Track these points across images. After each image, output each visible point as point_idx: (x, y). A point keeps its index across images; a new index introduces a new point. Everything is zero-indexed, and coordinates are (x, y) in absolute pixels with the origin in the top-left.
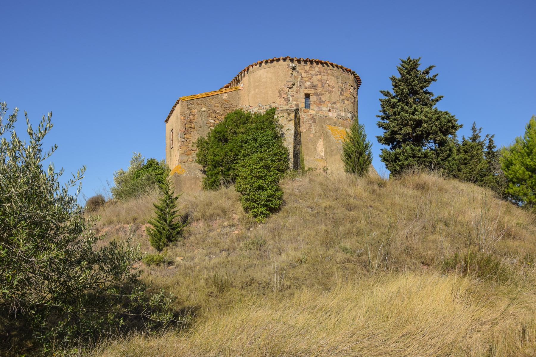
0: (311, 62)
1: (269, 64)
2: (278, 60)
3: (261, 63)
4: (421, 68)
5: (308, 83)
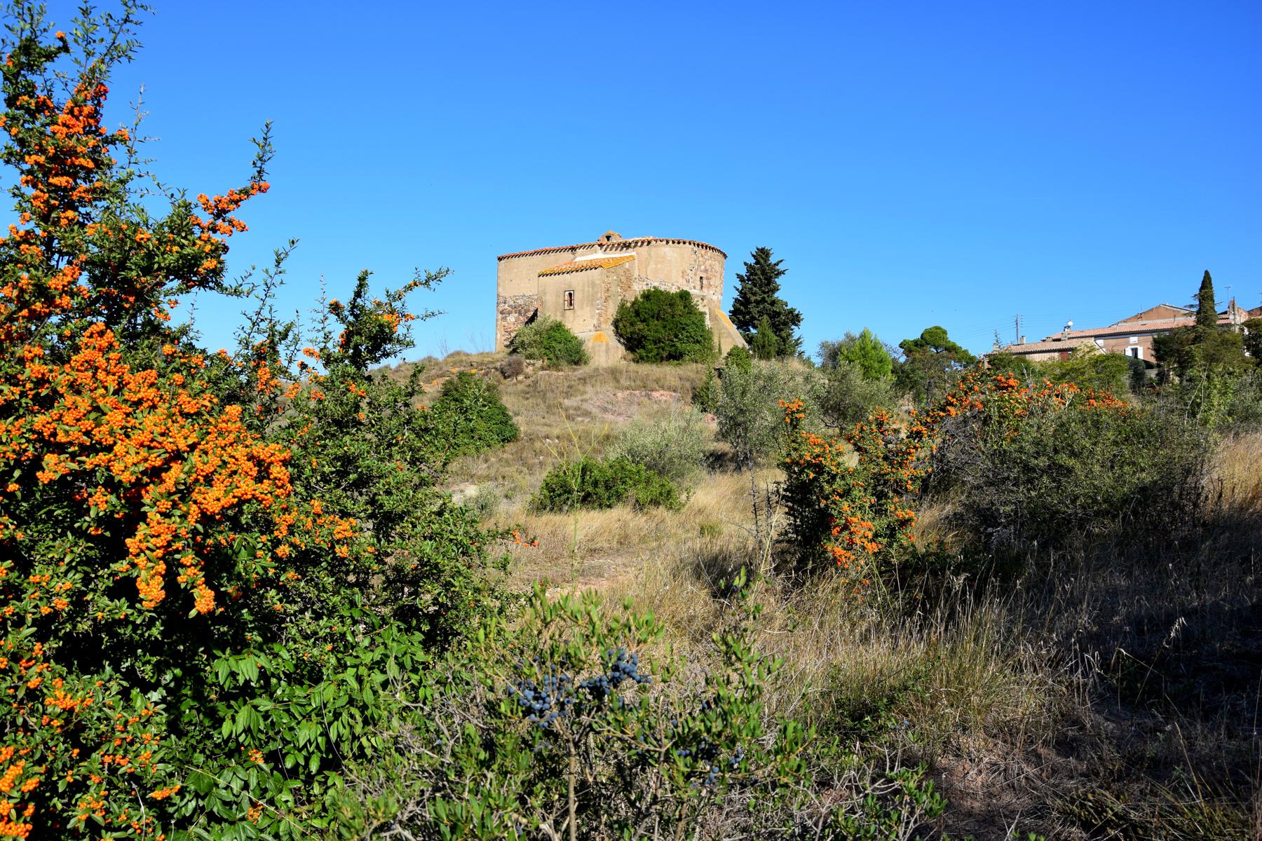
2: (684, 243)
3: (668, 242)
4: (773, 260)
5: (703, 267)
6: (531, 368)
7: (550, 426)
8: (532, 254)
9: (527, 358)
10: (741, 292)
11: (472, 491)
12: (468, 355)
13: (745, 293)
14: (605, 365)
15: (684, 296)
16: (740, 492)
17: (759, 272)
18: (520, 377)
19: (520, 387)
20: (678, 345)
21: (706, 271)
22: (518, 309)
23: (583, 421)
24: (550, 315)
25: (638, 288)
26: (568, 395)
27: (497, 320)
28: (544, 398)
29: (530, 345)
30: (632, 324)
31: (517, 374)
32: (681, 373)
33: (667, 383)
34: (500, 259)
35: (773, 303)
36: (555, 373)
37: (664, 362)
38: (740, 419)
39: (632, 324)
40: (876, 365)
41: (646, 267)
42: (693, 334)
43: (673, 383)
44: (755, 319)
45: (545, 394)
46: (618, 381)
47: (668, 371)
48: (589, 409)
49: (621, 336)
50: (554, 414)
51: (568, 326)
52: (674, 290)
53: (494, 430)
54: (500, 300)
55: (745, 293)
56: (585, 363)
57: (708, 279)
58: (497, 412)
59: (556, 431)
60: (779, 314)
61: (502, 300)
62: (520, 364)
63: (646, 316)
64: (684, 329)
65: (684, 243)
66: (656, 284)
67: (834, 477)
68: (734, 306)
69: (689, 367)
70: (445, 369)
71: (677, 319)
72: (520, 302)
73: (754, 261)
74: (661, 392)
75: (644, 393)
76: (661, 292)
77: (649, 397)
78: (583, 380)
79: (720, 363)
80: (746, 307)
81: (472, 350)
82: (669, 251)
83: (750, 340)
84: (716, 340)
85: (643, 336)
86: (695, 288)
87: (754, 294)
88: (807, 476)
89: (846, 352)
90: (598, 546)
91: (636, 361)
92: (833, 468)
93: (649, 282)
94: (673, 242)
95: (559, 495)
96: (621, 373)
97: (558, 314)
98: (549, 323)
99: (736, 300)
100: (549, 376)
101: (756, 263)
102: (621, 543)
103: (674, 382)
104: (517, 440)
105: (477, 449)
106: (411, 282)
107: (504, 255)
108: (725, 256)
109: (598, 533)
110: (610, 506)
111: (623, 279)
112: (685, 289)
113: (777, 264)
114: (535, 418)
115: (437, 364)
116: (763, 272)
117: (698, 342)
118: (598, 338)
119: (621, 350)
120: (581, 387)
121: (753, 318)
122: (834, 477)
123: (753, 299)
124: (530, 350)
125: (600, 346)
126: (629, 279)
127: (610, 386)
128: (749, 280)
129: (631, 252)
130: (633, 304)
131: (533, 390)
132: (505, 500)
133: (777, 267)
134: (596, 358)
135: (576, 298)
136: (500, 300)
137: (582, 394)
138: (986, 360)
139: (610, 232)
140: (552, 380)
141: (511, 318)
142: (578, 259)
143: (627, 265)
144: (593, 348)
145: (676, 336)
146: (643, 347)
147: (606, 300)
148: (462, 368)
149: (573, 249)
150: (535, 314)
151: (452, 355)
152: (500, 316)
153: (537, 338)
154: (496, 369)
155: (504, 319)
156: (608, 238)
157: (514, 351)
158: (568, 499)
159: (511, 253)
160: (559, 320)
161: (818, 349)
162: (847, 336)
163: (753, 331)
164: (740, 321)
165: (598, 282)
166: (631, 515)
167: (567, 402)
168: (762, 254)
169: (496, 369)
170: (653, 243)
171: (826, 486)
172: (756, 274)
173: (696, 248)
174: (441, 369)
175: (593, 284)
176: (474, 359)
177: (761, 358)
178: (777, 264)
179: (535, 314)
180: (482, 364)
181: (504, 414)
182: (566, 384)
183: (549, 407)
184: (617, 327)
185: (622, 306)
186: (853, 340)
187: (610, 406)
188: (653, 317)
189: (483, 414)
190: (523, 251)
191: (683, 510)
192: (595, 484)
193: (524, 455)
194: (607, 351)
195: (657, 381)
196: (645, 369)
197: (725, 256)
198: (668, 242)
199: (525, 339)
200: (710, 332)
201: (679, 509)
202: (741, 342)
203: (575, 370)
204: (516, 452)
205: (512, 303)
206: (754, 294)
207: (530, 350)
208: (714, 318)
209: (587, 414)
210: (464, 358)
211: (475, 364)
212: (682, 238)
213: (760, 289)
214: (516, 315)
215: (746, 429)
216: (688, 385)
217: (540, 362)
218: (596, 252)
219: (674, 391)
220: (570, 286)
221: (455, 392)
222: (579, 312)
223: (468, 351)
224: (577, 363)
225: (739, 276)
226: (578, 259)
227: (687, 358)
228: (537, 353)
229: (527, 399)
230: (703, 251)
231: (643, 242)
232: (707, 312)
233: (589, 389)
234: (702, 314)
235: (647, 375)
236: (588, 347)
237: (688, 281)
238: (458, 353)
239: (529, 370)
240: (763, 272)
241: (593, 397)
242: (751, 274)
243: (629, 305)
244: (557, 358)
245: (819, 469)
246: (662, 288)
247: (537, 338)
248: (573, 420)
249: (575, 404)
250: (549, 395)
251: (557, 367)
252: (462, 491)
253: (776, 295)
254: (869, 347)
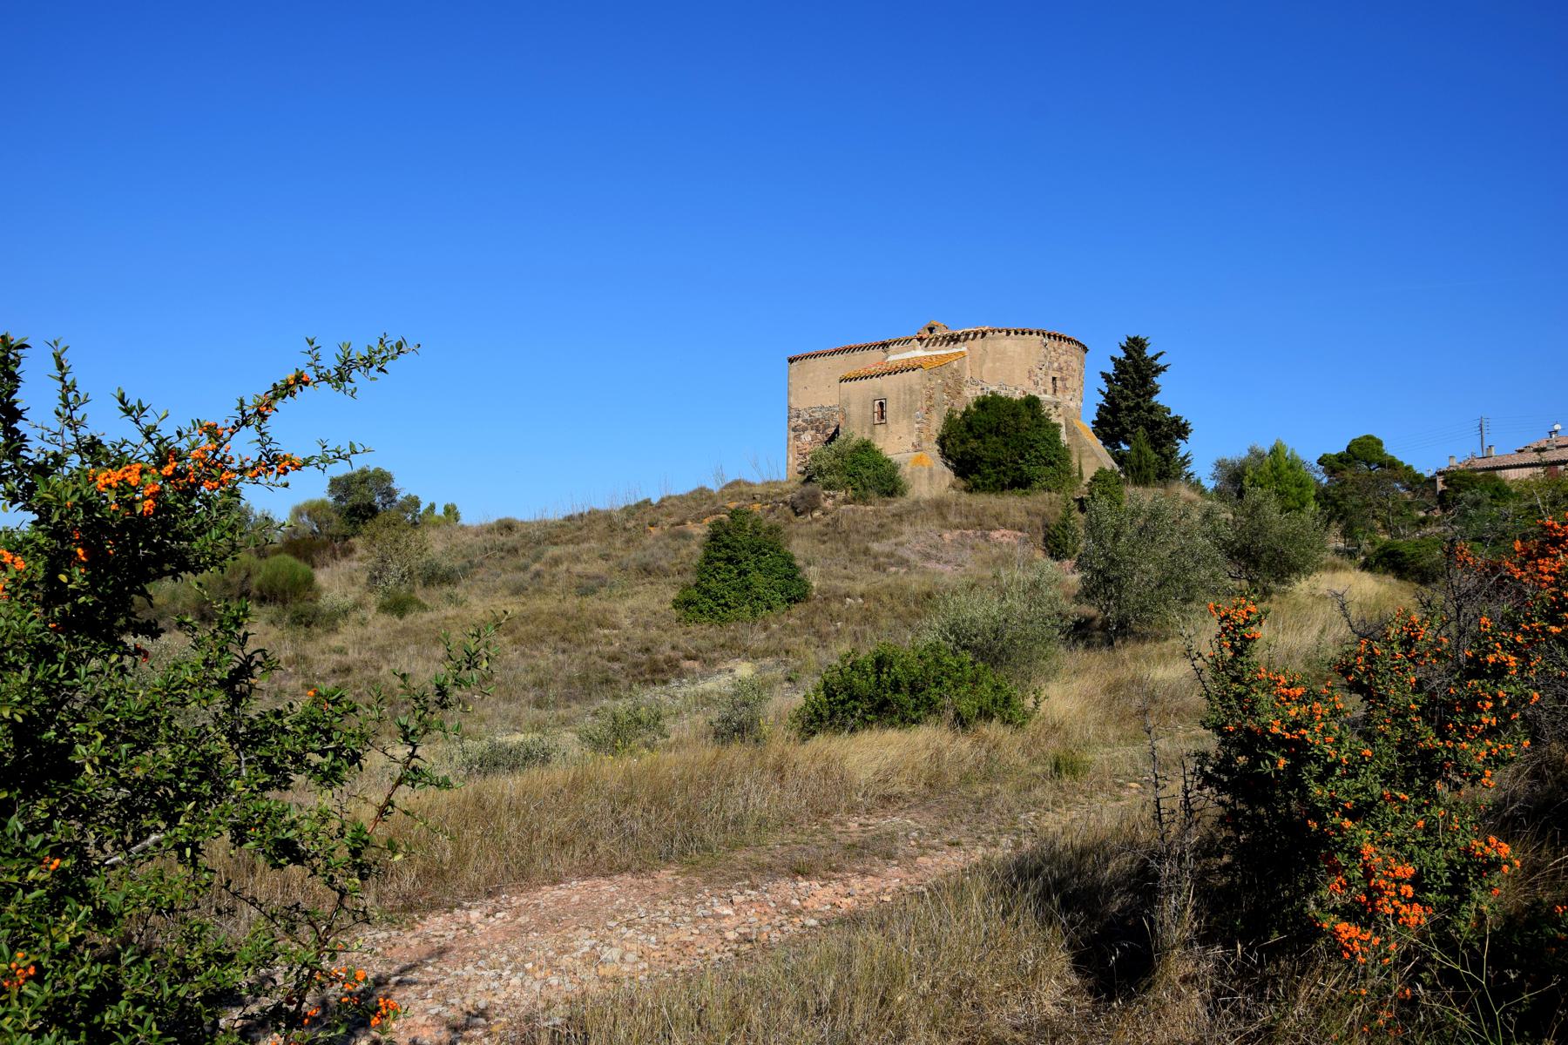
0: (1060, 337)
1: (1019, 335)
2: (1031, 333)
3: (1008, 333)
4: (1149, 352)
5: (1056, 365)
6: (830, 501)
7: (853, 579)
8: (832, 353)
9: (825, 488)
10: (1107, 396)
11: (744, 670)
12: (750, 485)
13: (1113, 398)
14: (927, 496)
15: (1032, 403)
16: (1114, 689)
17: (1131, 369)
18: (817, 514)
19: (817, 527)
20: (1025, 468)
21: (1060, 369)
23: (896, 573)
24: (856, 432)
25: (971, 394)
26: (877, 536)
27: (788, 439)
28: (846, 542)
29: (829, 471)
30: (963, 442)
31: (813, 509)
32: (1030, 505)
33: (1010, 520)
34: (791, 361)
35: (1152, 409)
36: (862, 507)
37: (1006, 491)
38: (1113, 574)
39: (963, 442)
40: (1294, 490)
41: (981, 366)
42: (1044, 453)
43: (1018, 519)
44: (1127, 431)
45: (848, 536)
46: (945, 518)
47: (1012, 504)
48: (906, 556)
49: (949, 457)
50: (858, 563)
51: (878, 445)
52: (1018, 396)
53: (777, 587)
54: (792, 413)
55: (1113, 398)
56: (902, 494)
57: (1063, 379)
58: (781, 562)
59: (860, 587)
60: (1159, 424)
61: (794, 413)
62: (815, 496)
63: (982, 431)
64: (1031, 447)
65: (1031, 333)
66: (994, 388)
67: (1330, 769)
68: (1098, 415)
69: (1040, 498)
70: (720, 503)
71: (1022, 433)
72: (818, 415)
73: (1124, 355)
74: (1003, 531)
75: (979, 533)
76: (1001, 399)
77: (985, 537)
78: (899, 517)
79: (1082, 491)
80: (1115, 416)
81: (756, 479)
82: (1011, 345)
83: (1120, 459)
84: (1075, 460)
85: (980, 459)
86: (1045, 392)
87: (1126, 399)
88: (1274, 763)
89: (1251, 474)
90: (896, 789)
91: (969, 490)
92: (1328, 748)
93: (984, 385)
94: (1016, 333)
95: (843, 702)
96: (949, 506)
97: (866, 430)
98: (854, 441)
99: (1101, 407)
100: (854, 512)
101: (1127, 358)
102: (931, 785)
103: (1020, 518)
104: (808, 600)
105: (754, 613)
106: (291, 376)
107: (796, 354)
108: (1085, 349)
109: (894, 770)
110: (916, 722)
111: (950, 382)
112: (1033, 393)
113: (1155, 358)
114: (833, 568)
115: (710, 497)
116: (1137, 369)
117: (1051, 463)
118: (918, 460)
119: (949, 476)
120: (895, 526)
121: (1124, 431)
122: (1330, 769)
123: (1124, 404)
124: (829, 478)
125: (920, 471)
126: (959, 382)
127: (934, 525)
128: (1118, 379)
129: (961, 348)
130: (964, 415)
131: (833, 531)
132: (786, 685)
133: (1156, 362)
134: (916, 486)
135: (890, 409)
136: (792, 413)
137: (896, 536)
138: (1440, 479)
139: (934, 322)
140: (858, 517)
141: (807, 437)
142: (891, 358)
143: (955, 365)
144: (912, 473)
145: (1022, 457)
146: (979, 472)
147: (928, 410)
148: (742, 502)
149: (885, 345)
150: (837, 431)
151: (730, 485)
152: (792, 434)
153: (838, 461)
154: (785, 503)
155: (797, 438)
156: (931, 330)
157: (809, 479)
158: (855, 708)
159: (806, 352)
160: (866, 438)
161: (1212, 470)
162: (1252, 451)
163: (1125, 447)
164: (1106, 434)
165: (917, 387)
166: (949, 736)
167: (876, 547)
168: (1135, 346)
169: (785, 503)
171: (1316, 790)
172: (1127, 372)
173: (1046, 340)
174: (714, 503)
175: (911, 391)
176: (758, 490)
177: (1136, 483)
178: (1155, 358)
179: (837, 431)
180: (767, 496)
181: (791, 565)
182: (877, 522)
183: (853, 553)
184: (943, 445)
185: (950, 418)
186: (1260, 456)
187: (934, 552)
188: (990, 431)
189: (763, 565)
190: (820, 350)
191: (1029, 726)
192: (896, 686)
193: (817, 620)
194: (931, 476)
195: (997, 517)
196: (981, 500)
197: (1085, 349)
198: (1008, 333)
199: (822, 463)
200: (1067, 450)
201: (1022, 724)
202: (1109, 463)
203: (888, 503)
204: (805, 616)
205: (807, 417)
206: (1126, 399)
207: (829, 478)
208: (1073, 432)
209: (903, 562)
210: (745, 489)
211: (758, 497)
212: (1028, 327)
213: (1133, 391)
214: (813, 432)
215: (1120, 588)
216: (1038, 521)
217: (843, 493)
219: (1020, 530)
220: (881, 393)
221: (725, 537)
222: (893, 427)
223: (750, 479)
224: (891, 494)
225: (1105, 376)
226: (891, 358)
227: (1037, 485)
228: (839, 482)
229: (824, 542)
230: (1056, 344)
231: (976, 334)
232: (1063, 423)
233: (906, 528)
234: (1056, 426)
235: (984, 509)
236: (905, 472)
237: (1036, 384)
238: (737, 483)
239: (829, 504)
240: (1137, 369)
241: (912, 539)
242: (1121, 372)
243: (958, 416)
244: (865, 488)
245: (1299, 752)
246: (1003, 393)
247: (838, 461)
248: (885, 570)
249: (887, 549)
250: (854, 536)
251: (865, 500)
252: (731, 671)
253: (1155, 399)
254: (1284, 467)
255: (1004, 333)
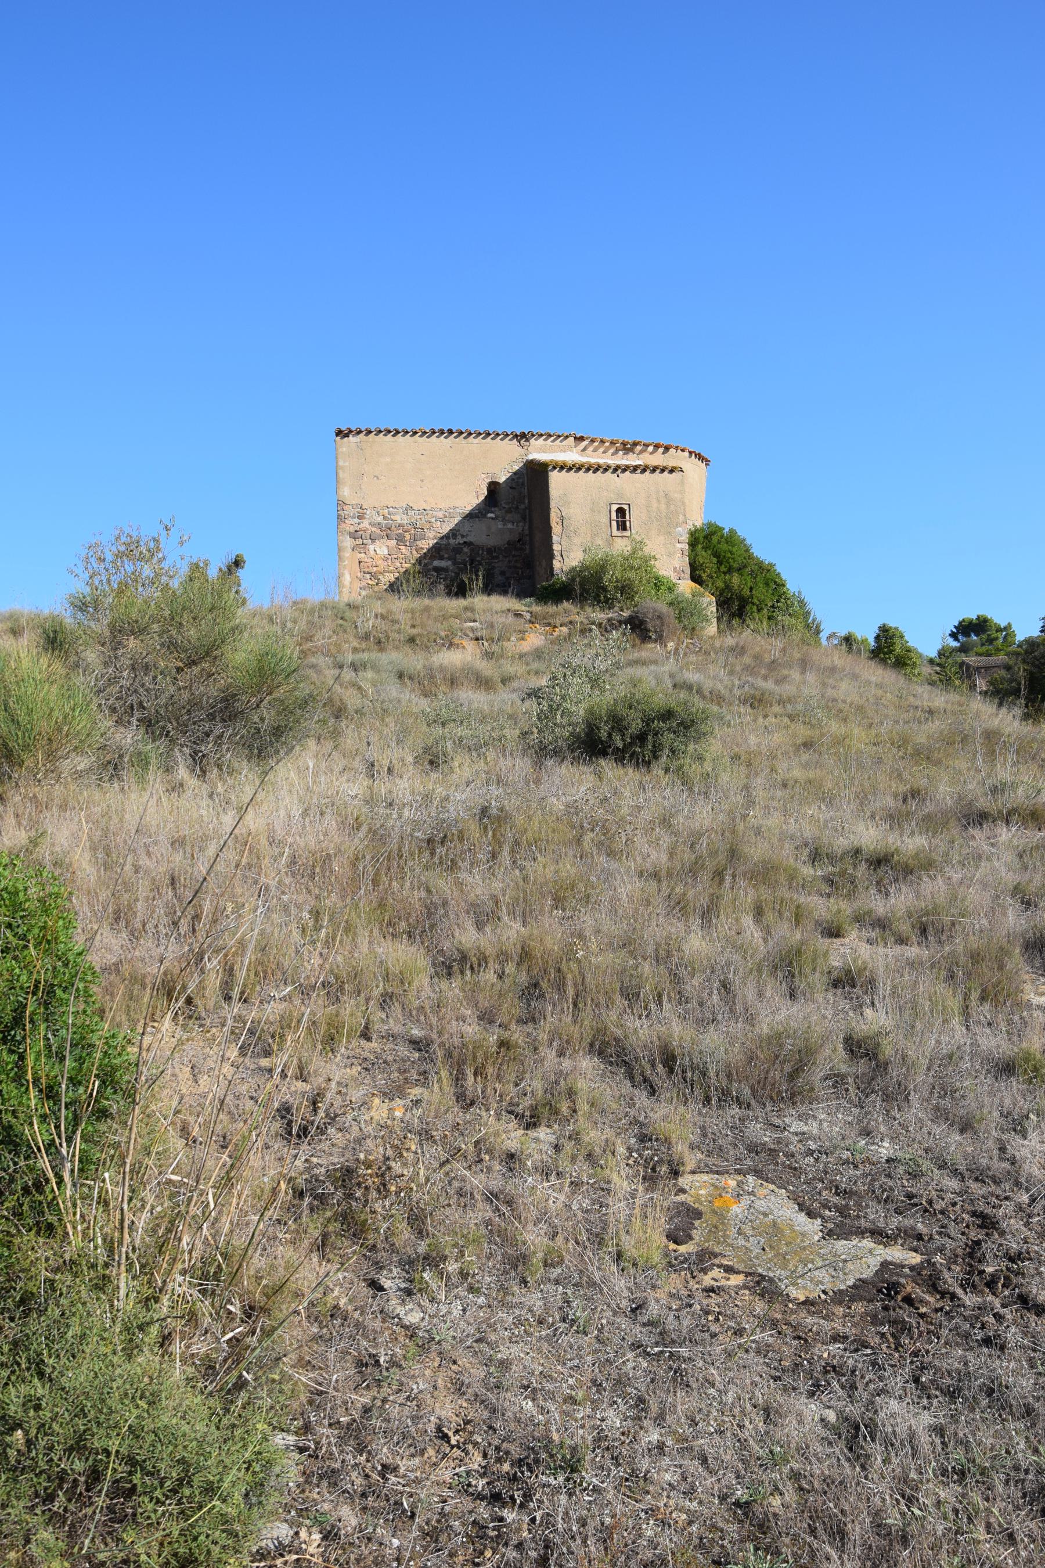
22: (387, 531)
34: (339, 433)
72: (399, 518)
135: (634, 518)
141: (381, 548)
149: (522, 437)
152: (348, 542)
170: (672, 451)
175: (668, 499)
198: (690, 453)
205: (380, 519)
214: (394, 542)
218: (570, 448)
255: (687, 454)
